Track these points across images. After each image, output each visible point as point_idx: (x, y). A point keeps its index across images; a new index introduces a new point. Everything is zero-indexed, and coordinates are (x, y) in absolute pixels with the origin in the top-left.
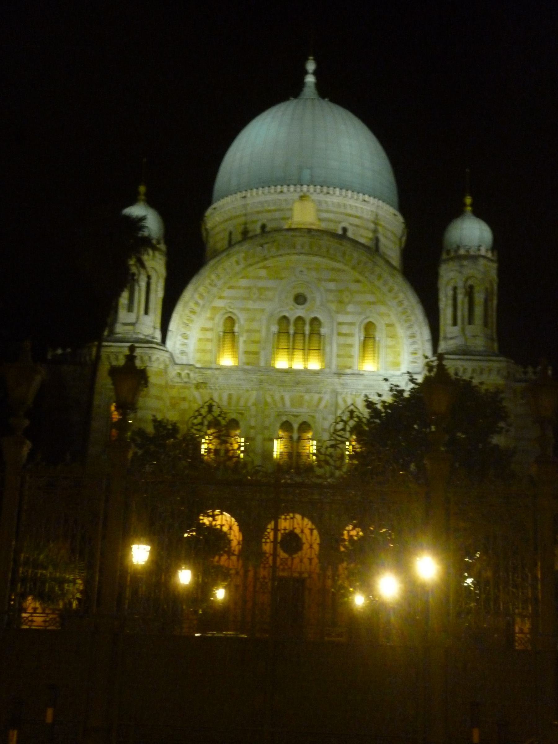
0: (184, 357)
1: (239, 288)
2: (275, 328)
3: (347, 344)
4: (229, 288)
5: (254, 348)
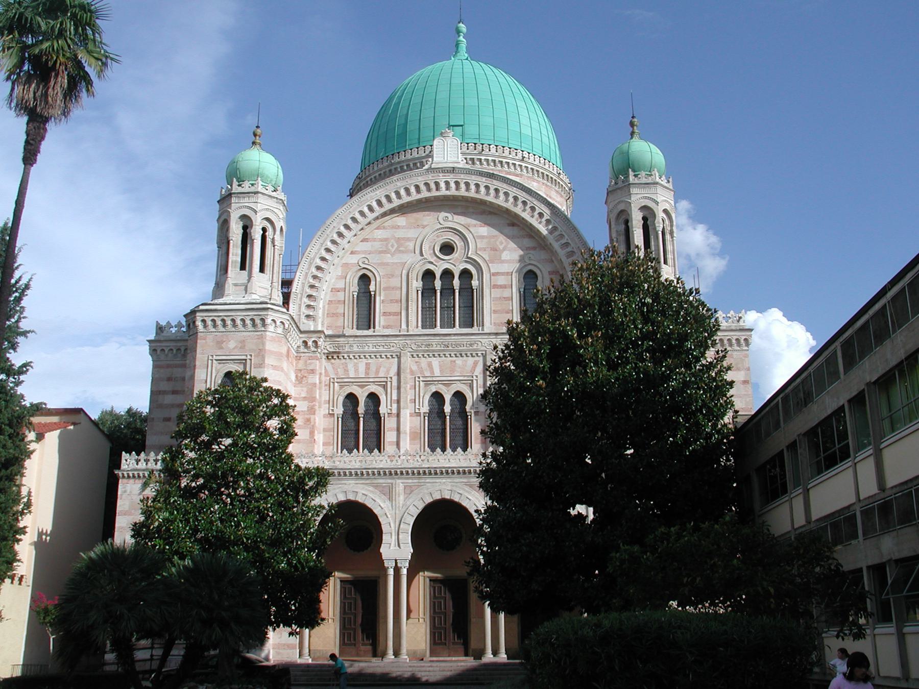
0: (311, 323)
1: (374, 240)
2: (417, 284)
3: (504, 298)
4: (361, 241)
5: (395, 308)
